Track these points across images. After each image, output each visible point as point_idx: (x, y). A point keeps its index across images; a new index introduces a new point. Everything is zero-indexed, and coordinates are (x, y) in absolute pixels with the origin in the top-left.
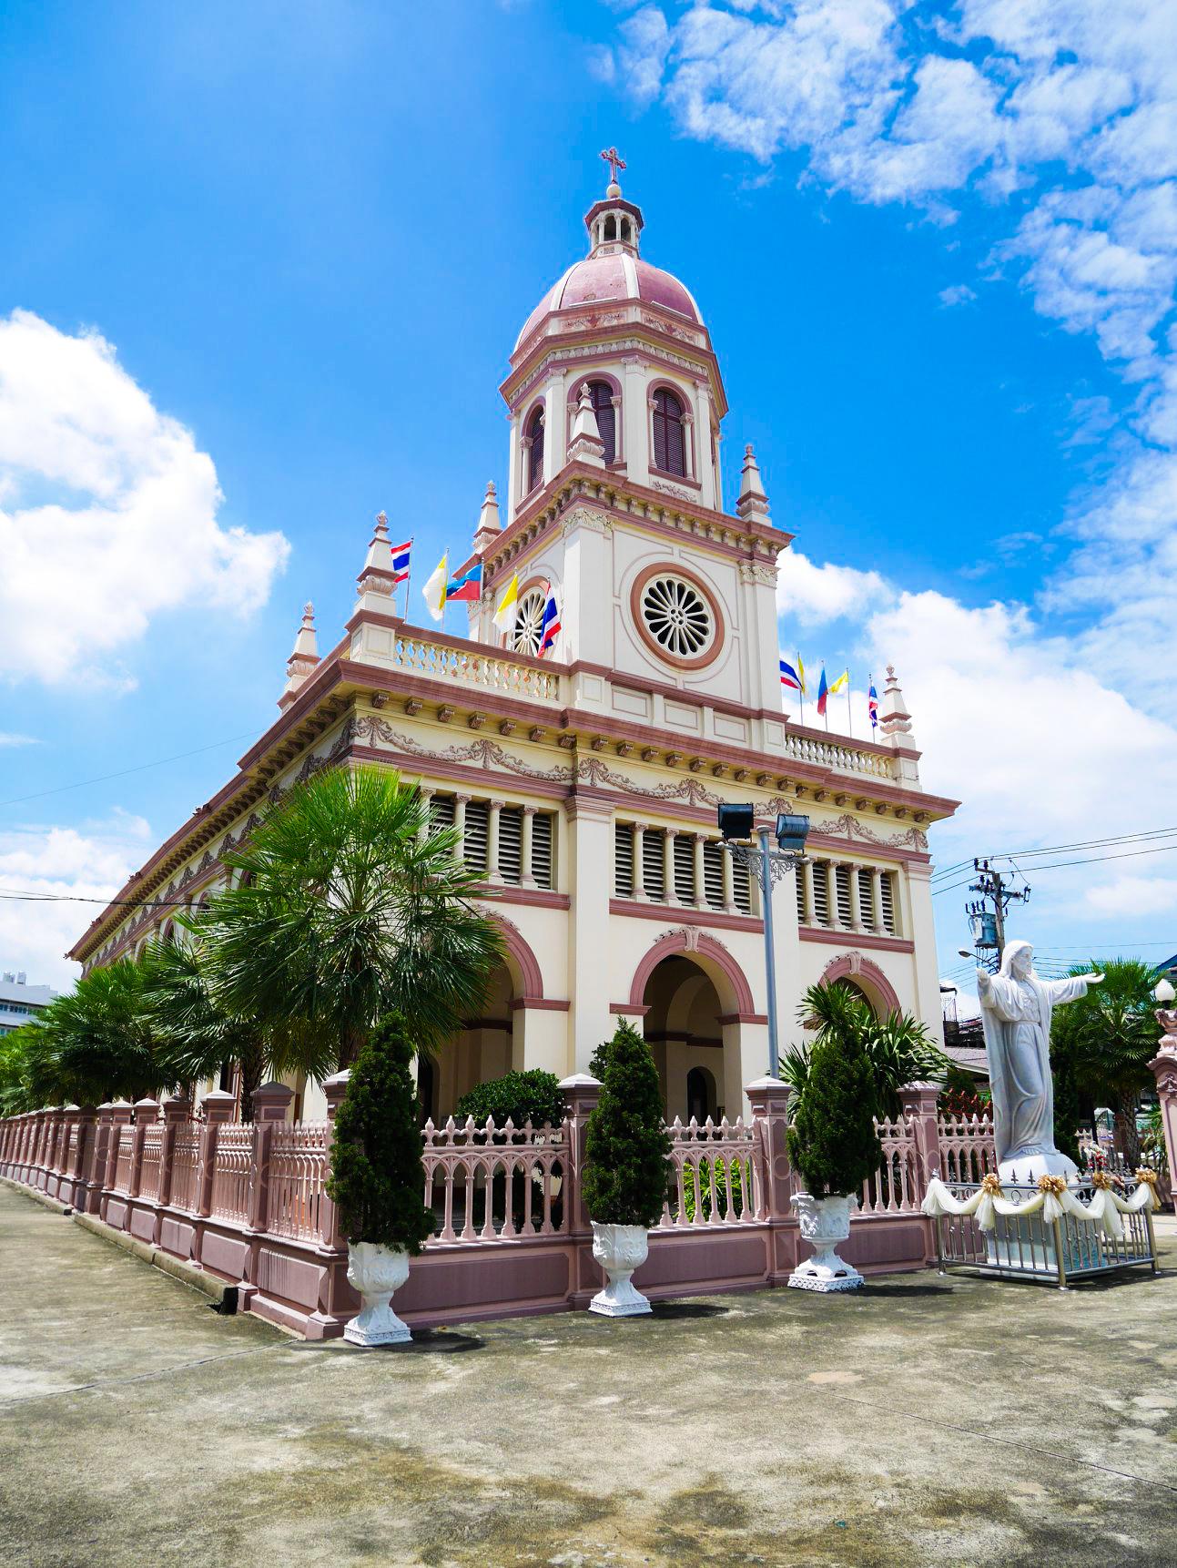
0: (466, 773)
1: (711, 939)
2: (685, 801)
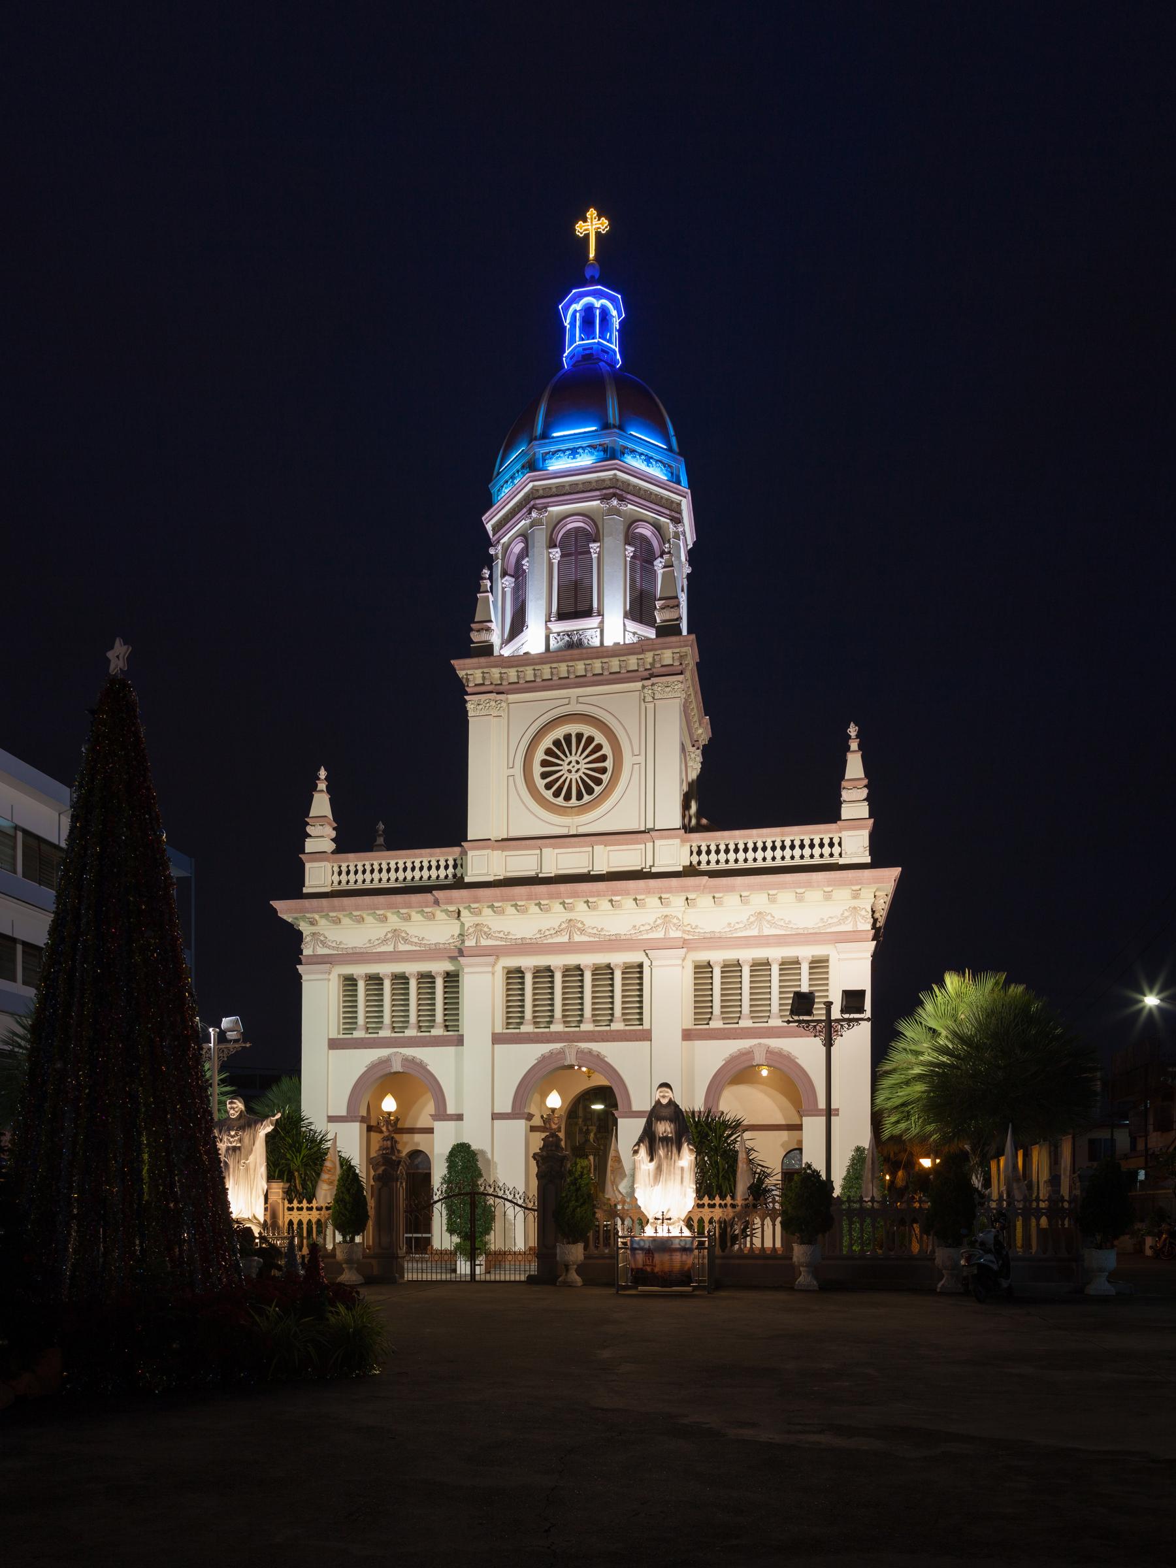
0: (381, 958)
1: (590, 1052)
2: (564, 939)
